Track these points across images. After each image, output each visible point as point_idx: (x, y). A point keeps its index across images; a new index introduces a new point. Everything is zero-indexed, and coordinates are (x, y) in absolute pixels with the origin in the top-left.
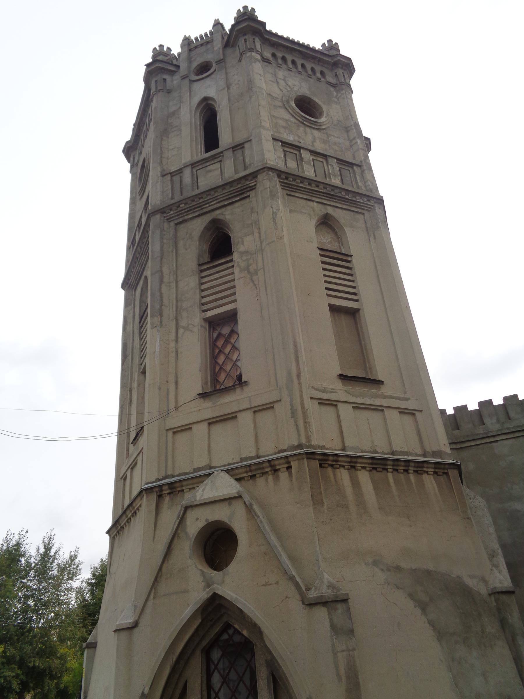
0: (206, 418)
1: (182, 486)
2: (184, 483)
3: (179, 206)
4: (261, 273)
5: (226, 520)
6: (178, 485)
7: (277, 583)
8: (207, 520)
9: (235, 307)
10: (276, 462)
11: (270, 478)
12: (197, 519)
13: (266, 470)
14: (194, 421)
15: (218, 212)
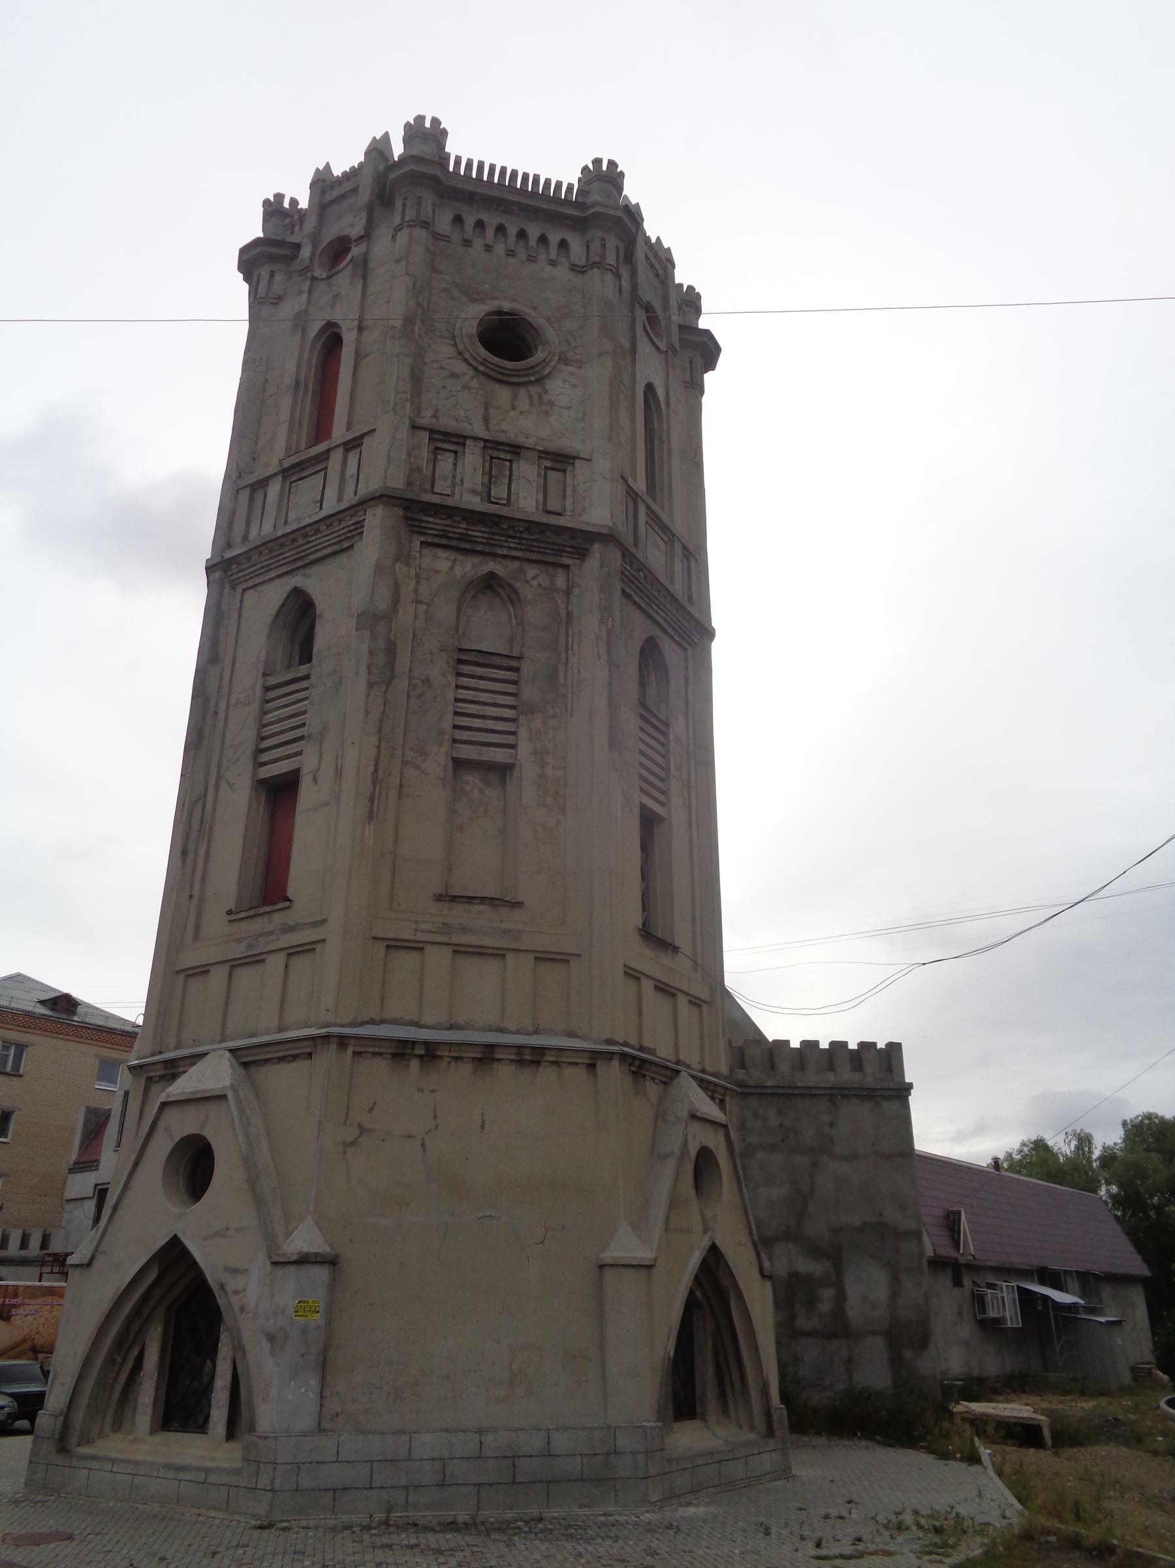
2: (653, 1068)
3: (638, 570)
4: (693, 793)
14: (646, 972)
15: (658, 633)
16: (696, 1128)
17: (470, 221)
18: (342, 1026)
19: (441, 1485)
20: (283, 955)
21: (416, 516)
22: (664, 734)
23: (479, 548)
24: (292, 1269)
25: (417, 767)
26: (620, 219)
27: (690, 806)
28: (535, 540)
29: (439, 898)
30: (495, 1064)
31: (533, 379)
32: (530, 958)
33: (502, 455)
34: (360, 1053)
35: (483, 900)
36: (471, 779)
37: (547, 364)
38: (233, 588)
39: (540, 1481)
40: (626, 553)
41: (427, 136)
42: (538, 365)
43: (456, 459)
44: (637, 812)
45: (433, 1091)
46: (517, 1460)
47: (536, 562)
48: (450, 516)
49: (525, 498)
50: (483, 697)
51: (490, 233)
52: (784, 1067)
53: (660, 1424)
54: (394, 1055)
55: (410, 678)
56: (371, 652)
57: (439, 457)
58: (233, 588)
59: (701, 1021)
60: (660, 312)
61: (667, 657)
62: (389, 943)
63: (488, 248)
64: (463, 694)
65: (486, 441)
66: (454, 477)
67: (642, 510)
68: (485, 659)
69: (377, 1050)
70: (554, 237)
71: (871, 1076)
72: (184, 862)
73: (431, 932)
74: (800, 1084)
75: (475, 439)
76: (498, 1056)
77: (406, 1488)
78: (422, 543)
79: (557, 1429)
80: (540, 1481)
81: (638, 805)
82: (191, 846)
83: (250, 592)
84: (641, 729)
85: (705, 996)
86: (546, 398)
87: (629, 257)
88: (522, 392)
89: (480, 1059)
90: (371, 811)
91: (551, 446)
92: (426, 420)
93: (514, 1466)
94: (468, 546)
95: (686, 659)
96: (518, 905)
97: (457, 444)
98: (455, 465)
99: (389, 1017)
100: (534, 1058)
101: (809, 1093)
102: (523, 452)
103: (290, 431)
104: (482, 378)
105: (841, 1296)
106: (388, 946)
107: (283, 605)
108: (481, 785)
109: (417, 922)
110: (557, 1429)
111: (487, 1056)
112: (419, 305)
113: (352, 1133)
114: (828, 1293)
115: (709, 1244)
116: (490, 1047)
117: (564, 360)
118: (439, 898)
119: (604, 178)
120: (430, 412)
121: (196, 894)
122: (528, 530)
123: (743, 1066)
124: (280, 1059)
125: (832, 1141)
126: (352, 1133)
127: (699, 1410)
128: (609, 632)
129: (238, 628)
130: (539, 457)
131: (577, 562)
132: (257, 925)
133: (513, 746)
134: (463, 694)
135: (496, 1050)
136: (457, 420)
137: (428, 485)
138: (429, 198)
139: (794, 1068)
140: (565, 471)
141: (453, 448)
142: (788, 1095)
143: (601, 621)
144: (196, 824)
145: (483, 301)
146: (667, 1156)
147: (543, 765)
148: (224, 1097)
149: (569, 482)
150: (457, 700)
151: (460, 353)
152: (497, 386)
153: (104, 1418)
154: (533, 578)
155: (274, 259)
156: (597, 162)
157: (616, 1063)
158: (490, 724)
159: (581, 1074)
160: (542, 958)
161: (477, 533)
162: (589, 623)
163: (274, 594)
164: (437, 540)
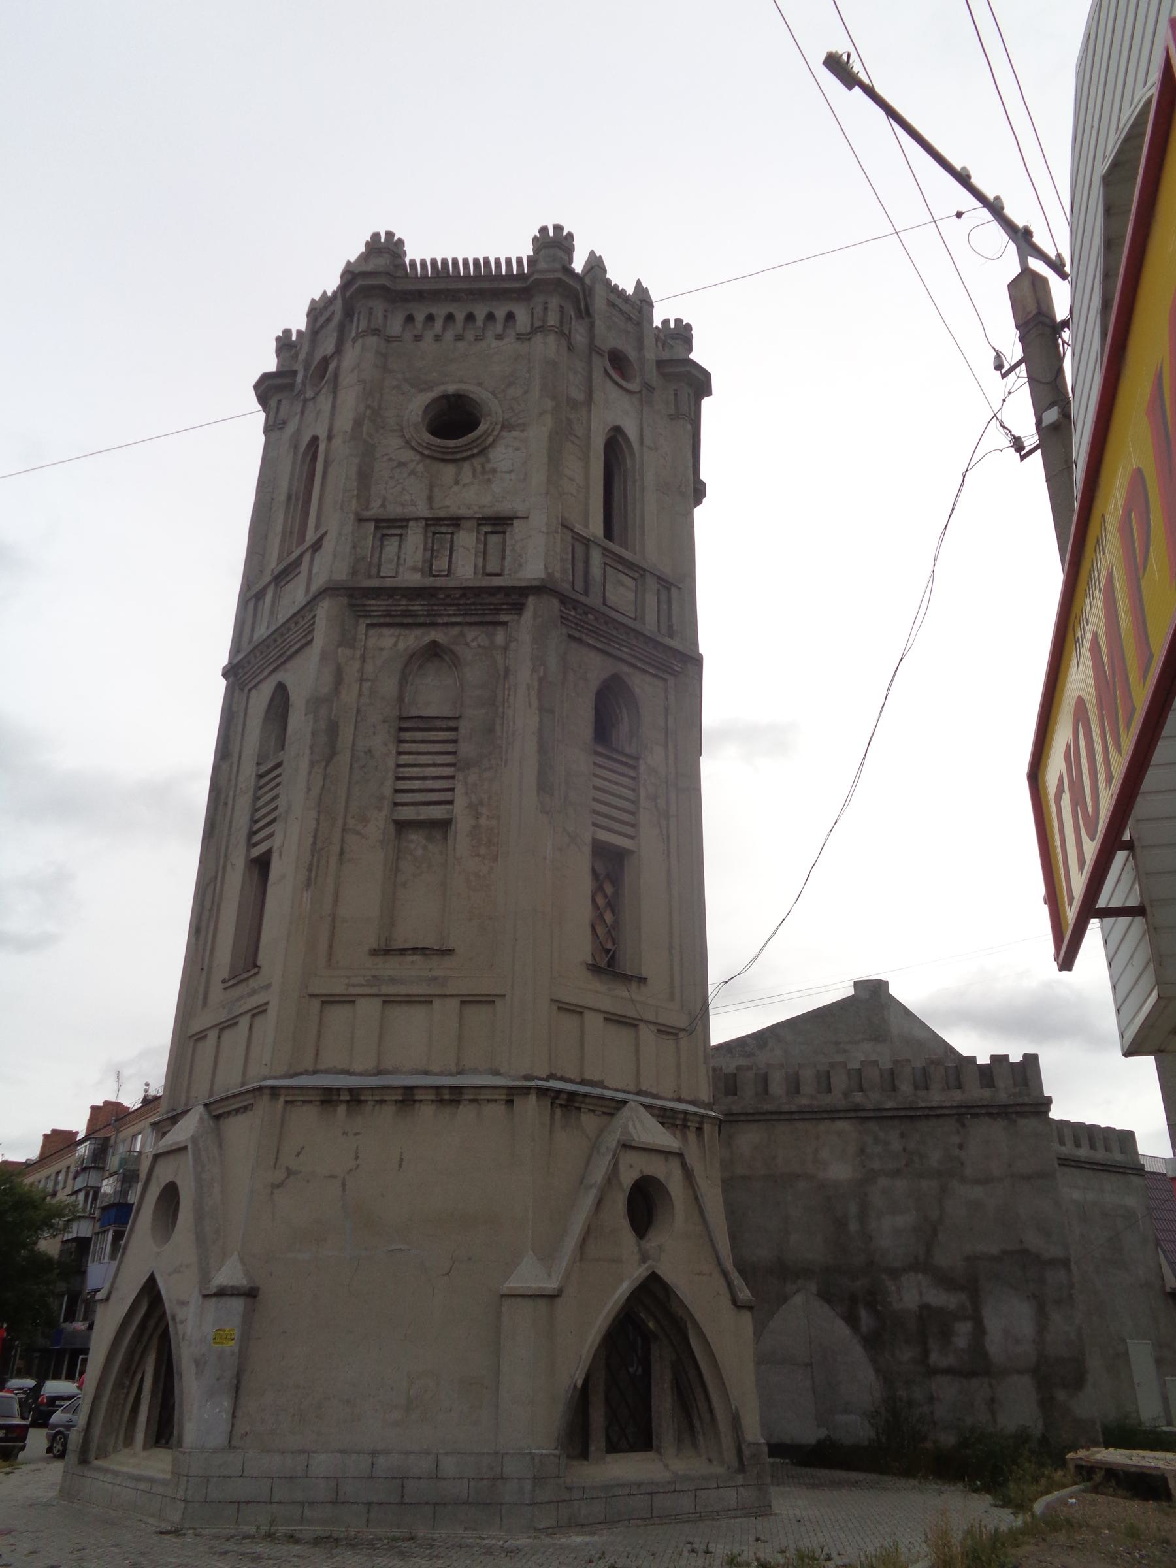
0: (603, 1008)
1: (582, 1102)
2: (588, 1100)
3: (586, 613)
5: (662, 1179)
6: (580, 1099)
7: (710, 1274)
8: (641, 1171)
9: (632, 848)
10: (691, 1117)
11: (678, 1133)
12: (631, 1166)
13: (678, 1122)
14: (590, 1006)
15: (625, 668)
16: (628, 1158)
17: (420, 317)
18: (275, 1078)
19: (334, 1503)
20: (249, 1015)
21: (359, 602)
22: (634, 768)
23: (422, 620)
24: (214, 1300)
25: (358, 833)
26: (559, 280)
27: (668, 837)
28: (474, 604)
29: (374, 953)
30: (417, 1105)
31: (475, 451)
32: (456, 1001)
33: (444, 529)
34: (292, 1102)
35: (415, 950)
36: (415, 838)
37: (490, 435)
38: (242, 690)
39: (427, 1503)
40: (564, 599)
41: (385, 249)
42: (481, 436)
43: (401, 541)
44: (587, 850)
45: (356, 1134)
46: (405, 1481)
47: (475, 624)
48: (391, 597)
49: (463, 566)
50: (423, 759)
51: (439, 324)
52: (905, 1088)
53: (557, 1452)
54: (323, 1102)
55: (353, 750)
56: (313, 734)
57: (386, 543)
58: (242, 690)
59: (678, 1050)
60: (632, 354)
61: (637, 690)
62: (324, 999)
63: (438, 338)
64: (404, 759)
65: (427, 519)
66: (399, 558)
67: (596, 557)
68: (426, 723)
69: (307, 1098)
70: (500, 314)
71: (1003, 1093)
72: (197, 939)
73: (362, 985)
74: (922, 1105)
75: (417, 519)
76: (417, 1097)
77: (303, 1504)
78: (368, 625)
79: (446, 1454)
80: (427, 1503)
81: (589, 840)
82: (204, 924)
83: (254, 691)
84: (595, 764)
85: (680, 1021)
86: (488, 466)
87: (585, 313)
88: (466, 466)
89: (402, 1101)
90: (309, 879)
91: (488, 512)
92: (375, 509)
93: (403, 1486)
94: (410, 620)
95: (666, 691)
96: (449, 952)
97: (402, 527)
98: (400, 547)
99: (322, 1067)
100: (453, 1097)
101: (934, 1114)
102: (462, 523)
103: (283, 541)
104: (428, 461)
105: (980, 1330)
106: (323, 1002)
107: (272, 699)
108: (424, 842)
109: (349, 977)
110: (446, 1454)
111: (408, 1098)
112: (368, 407)
113: (280, 1175)
114: (964, 1328)
115: (646, 1274)
116: (409, 1090)
117: (507, 426)
118: (374, 953)
119: (554, 244)
120: (379, 502)
121: (205, 968)
122: (464, 595)
123: (861, 1090)
124: (237, 1111)
125: (962, 1164)
126: (280, 1175)
127: (655, 1442)
128: (541, 680)
129: (244, 724)
130: (479, 525)
131: (516, 617)
132: (241, 990)
133: (451, 802)
134: (404, 759)
135: (416, 1091)
136: (403, 505)
137: (374, 571)
138: (379, 306)
139: (916, 1088)
140: (504, 533)
141: (398, 531)
142: (910, 1116)
143: (534, 670)
144: (208, 904)
145: (430, 389)
146: (591, 1187)
147: (477, 816)
148: (185, 1148)
149: (509, 542)
150: (399, 766)
151: (407, 442)
152: (441, 465)
153: (117, 1437)
154: (473, 640)
155: (280, 388)
156: (544, 230)
157: (533, 1098)
158: (430, 784)
159: (499, 1110)
160: (467, 1001)
161: (417, 607)
162: (524, 675)
163: (266, 690)
164: (382, 620)
